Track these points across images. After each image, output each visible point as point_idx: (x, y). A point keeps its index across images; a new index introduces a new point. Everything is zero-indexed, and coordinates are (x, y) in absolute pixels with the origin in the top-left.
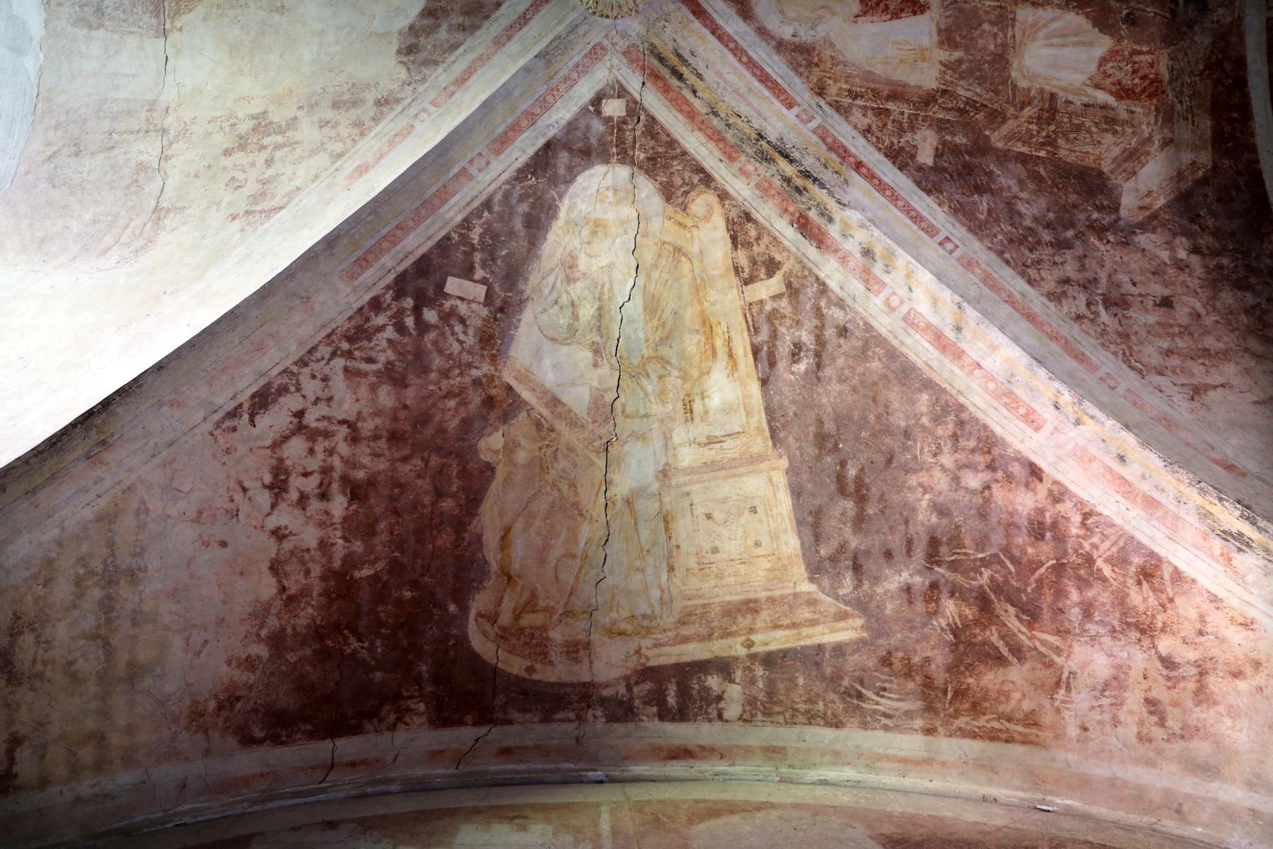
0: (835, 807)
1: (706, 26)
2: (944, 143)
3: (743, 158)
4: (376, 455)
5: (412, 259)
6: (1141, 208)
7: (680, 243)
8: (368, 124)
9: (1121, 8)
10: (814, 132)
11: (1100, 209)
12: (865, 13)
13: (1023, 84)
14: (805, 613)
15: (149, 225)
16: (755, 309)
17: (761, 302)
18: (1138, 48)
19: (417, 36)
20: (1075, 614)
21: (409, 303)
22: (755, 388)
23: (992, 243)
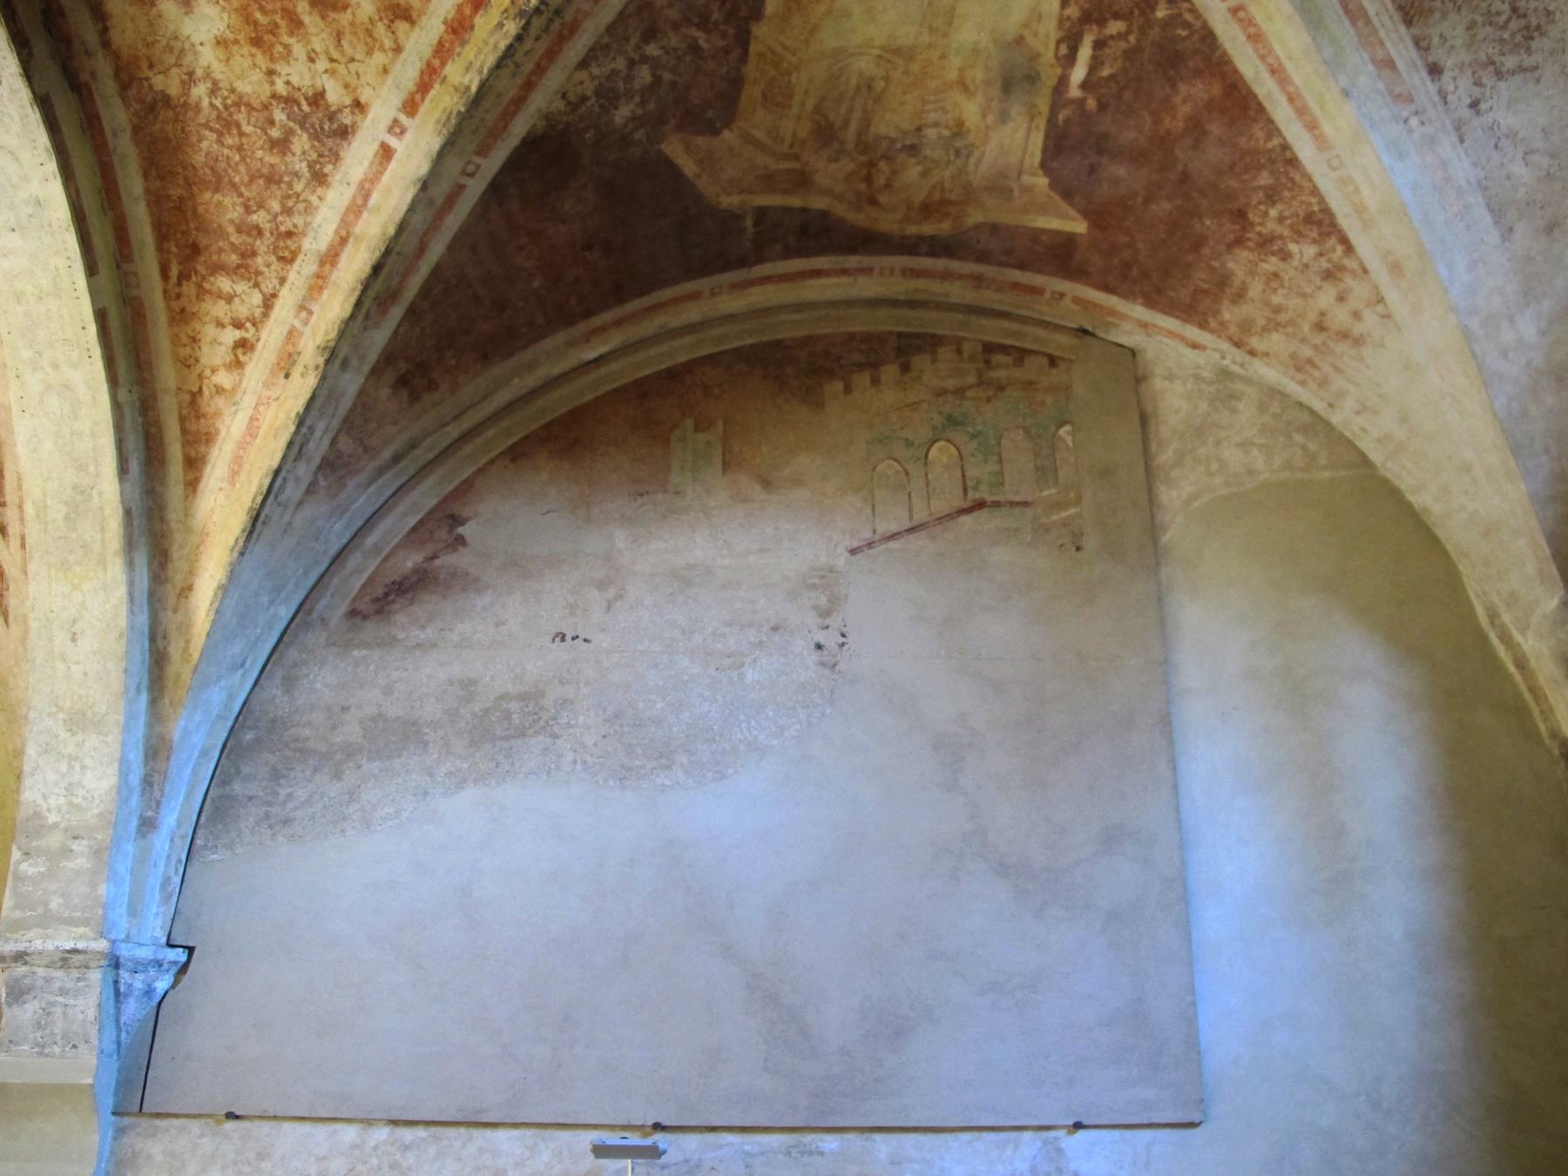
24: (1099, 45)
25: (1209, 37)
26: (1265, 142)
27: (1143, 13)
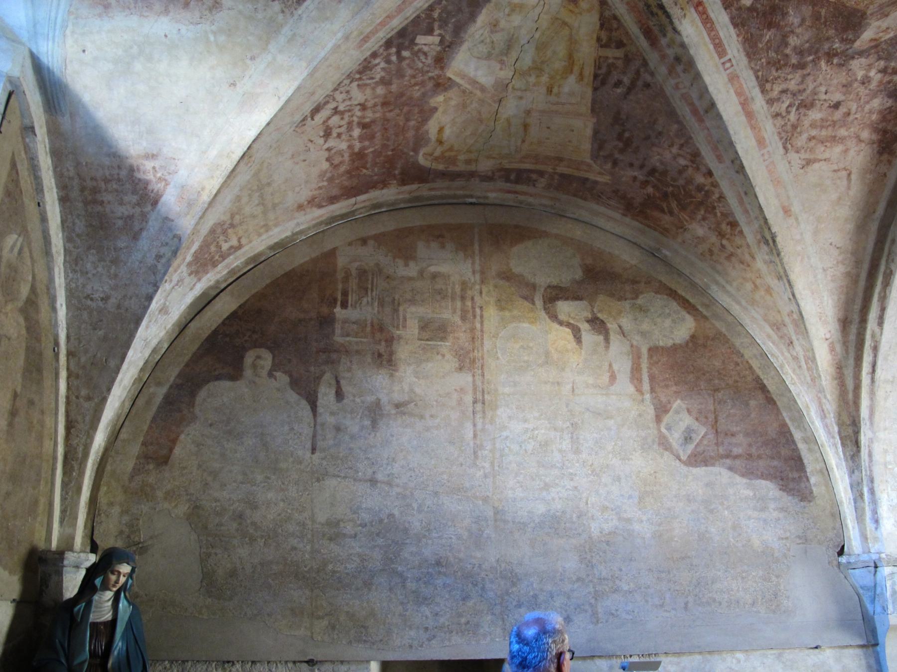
0: (572, 239)
4: (374, 112)
5: (396, 31)
16: (602, 60)
17: (607, 58)
20: (699, 217)
21: (394, 50)
22: (589, 92)
23: (756, 65)
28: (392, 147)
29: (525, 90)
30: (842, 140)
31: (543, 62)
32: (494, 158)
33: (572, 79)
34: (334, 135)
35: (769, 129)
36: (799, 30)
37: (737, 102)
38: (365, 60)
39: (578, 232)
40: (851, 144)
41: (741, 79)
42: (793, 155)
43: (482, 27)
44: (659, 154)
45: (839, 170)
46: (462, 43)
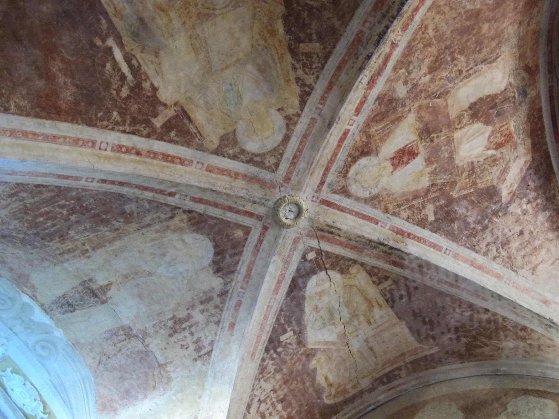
0: (443, 396)
1: (334, 208)
2: (436, 207)
3: (366, 250)
4: (282, 390)
6: (509, 194)
7: (351, 283)
8: (221, 305)
9: (494, 112)
10: (389, 229)
11: (495, 203)
12: (395, 169)
13: (460, 164)
14: (420, 351)
15: (162, 372)
17: (385, 288)
18: (502, 124)
19: (218, 264)
20: (503, 337)
21: (272, 352)
22: (390, 310)
23: (462, 242)
24: (123, 78)
25: (91, 123)
26: (15, 102)
27: (121, 108)
28: (305, 404)
29: (356, 330)
30: (541, 246)
31: (355, 311)
32: (366, 376)
33: (376, 310)
34: (267, 415)
35: (497, 267)
36: (469, 214)
37: (468, 266)
38: (260, 365)
39: (444, 389)
40: (548, 245)
41: (460, 254)
42: (521, 272)
43: (311, 313)
44: (452, 318)
45: (554, 262)
46: (305, 328)
